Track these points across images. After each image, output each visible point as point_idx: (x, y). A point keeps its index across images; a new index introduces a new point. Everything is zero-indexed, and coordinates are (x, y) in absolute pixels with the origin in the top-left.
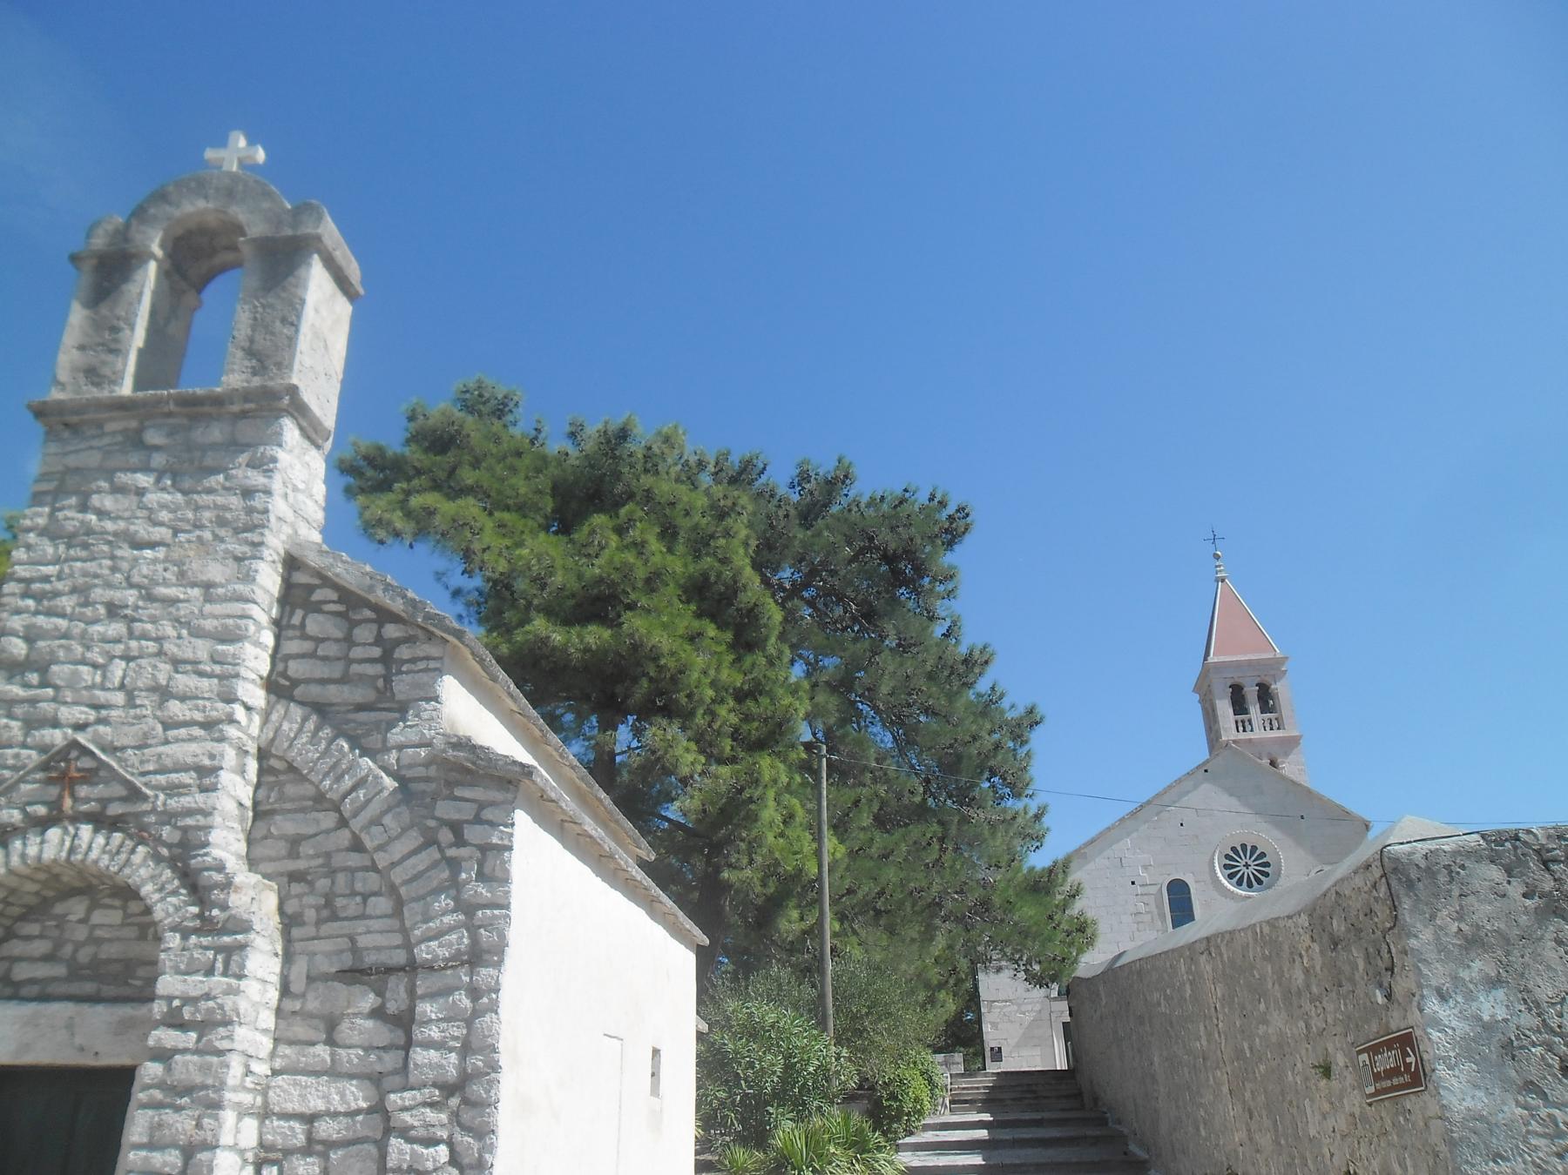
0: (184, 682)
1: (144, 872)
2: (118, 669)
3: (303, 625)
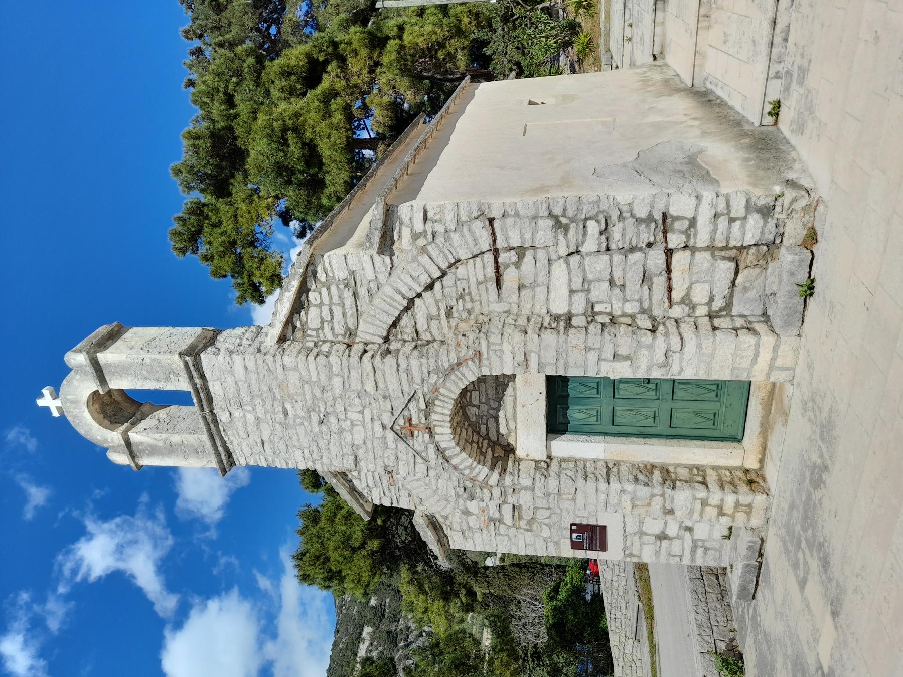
0: (356, 386)
2: (353, 415)
3: (317, 330)
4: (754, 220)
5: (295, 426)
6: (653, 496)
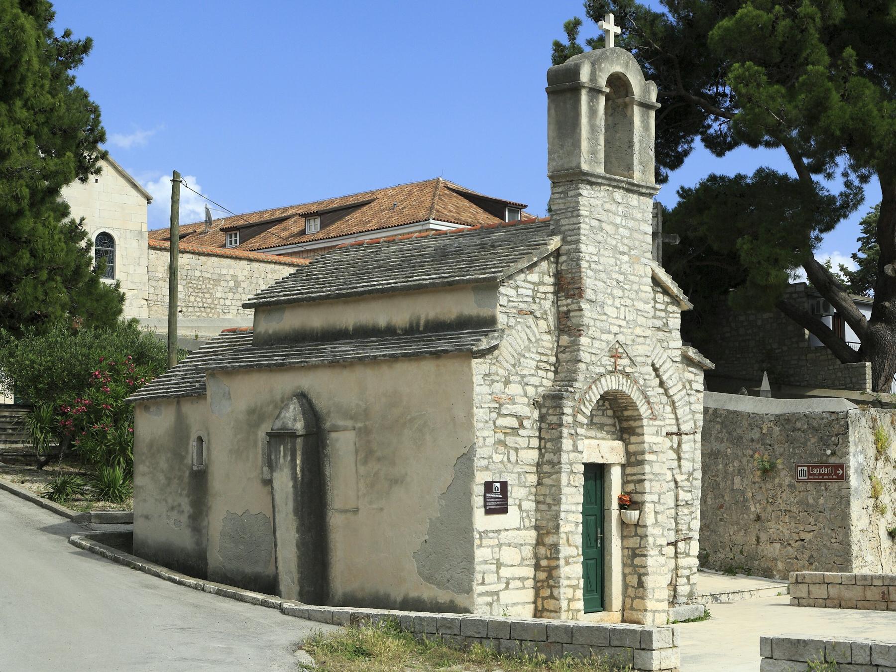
1: (636, 396)
5: (616, 258)
6: (577, 547)
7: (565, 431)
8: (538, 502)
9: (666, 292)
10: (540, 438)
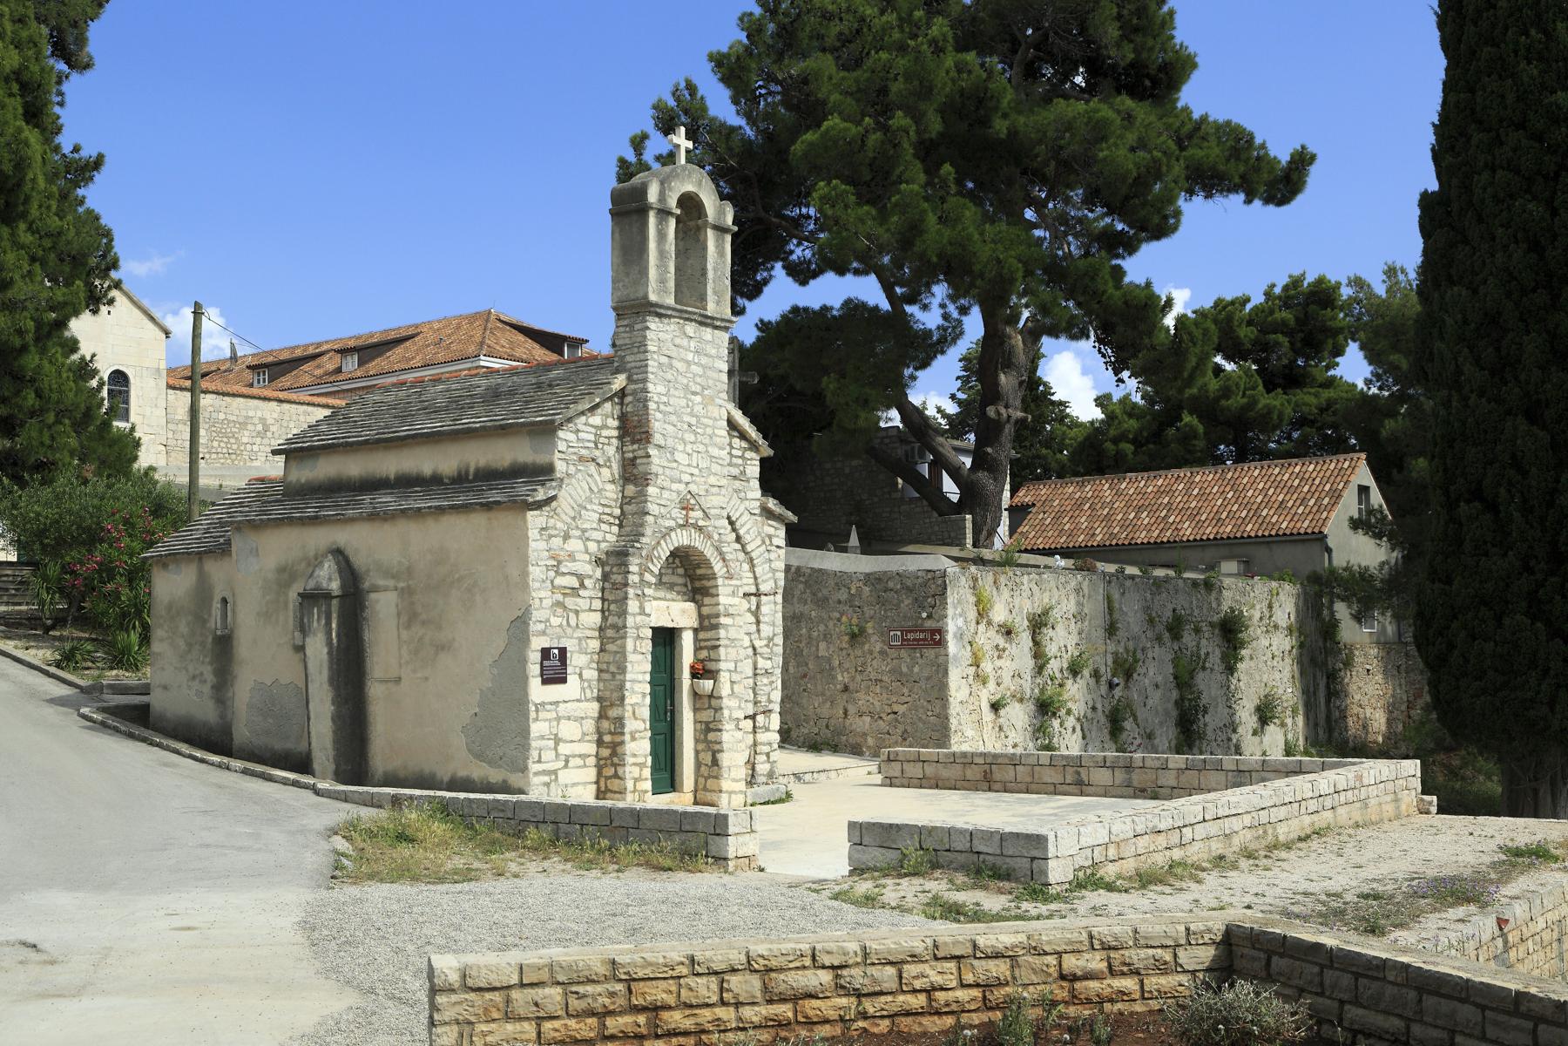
1: (709, 553)
4: (767, 767)
7: (631, 592)
8: (600, 671)
9: (743, 436)
10: (603, 599)
